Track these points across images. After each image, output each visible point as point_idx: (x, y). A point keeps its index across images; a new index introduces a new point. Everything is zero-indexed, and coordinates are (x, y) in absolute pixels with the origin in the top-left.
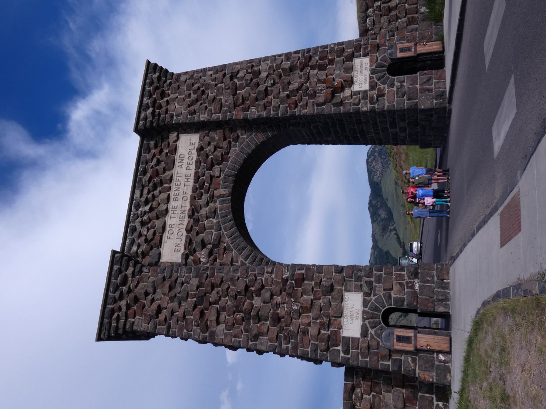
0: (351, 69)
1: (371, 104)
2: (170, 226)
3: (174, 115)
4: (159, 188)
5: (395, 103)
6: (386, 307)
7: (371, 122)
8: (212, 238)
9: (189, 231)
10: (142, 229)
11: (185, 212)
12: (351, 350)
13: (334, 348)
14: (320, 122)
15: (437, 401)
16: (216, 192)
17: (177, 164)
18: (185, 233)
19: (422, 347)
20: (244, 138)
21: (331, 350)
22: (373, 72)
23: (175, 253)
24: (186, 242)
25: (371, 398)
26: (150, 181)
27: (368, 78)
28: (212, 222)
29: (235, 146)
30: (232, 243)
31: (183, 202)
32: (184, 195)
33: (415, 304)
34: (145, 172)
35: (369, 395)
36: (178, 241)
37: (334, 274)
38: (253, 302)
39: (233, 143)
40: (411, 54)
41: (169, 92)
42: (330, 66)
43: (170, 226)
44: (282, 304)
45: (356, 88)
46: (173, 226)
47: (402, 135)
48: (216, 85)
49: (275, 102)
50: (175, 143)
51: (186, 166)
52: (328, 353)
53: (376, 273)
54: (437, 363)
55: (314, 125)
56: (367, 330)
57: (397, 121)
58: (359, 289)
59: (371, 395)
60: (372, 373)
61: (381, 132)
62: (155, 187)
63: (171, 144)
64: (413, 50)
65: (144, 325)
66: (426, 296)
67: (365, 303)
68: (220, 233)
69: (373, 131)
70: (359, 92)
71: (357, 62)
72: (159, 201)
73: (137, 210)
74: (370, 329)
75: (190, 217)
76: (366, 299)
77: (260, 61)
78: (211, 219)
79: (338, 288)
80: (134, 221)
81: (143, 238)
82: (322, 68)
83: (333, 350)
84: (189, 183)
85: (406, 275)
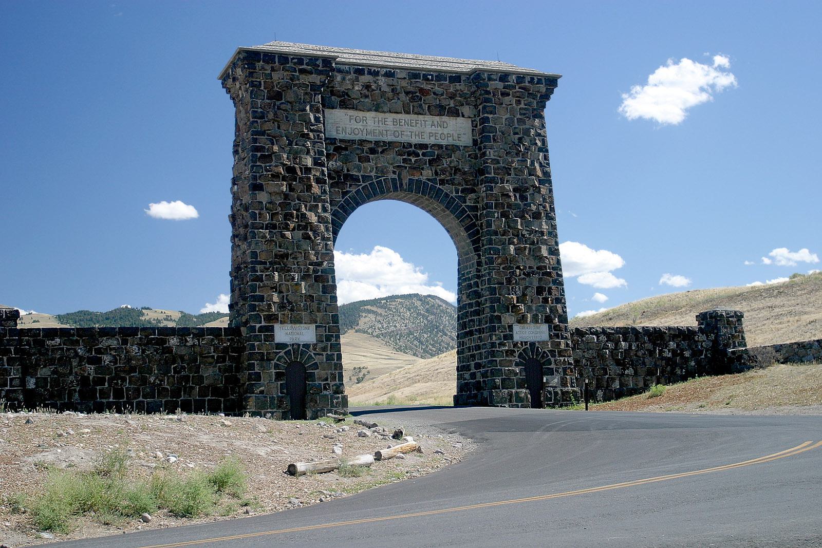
0: (535, 320)
1: (499, 344)
2: (365, 118)
3: (493, 115)
5: (499, 367)
7: (481, 344)
8: (354, 173)
11: (381, 136)
12: (263, 334)
16: (405, 171)
17: (437, 118)
18: (357, 138)
22: (532, 344)
23: (335, 128)
28: (371, 171)
29: (457, 192)
30: (349, 197)
31: (393, 132)
32: (400, 133)
35: (214, 352)
36: (348, 130)
37: (331, 314)
42: (541, 300)
43: (365, 118)
44: (297, 262)
45: (517, 328)
46: (364, 121)
47: (467, 376)
48: (526, 167)
49: (504, 240)
50: (461, 114)
51: (434, 132)
53: (334, 354)
54: (263, 412)
55: (480, 283)
56: (283, 349)
58: (319, 340)
59: (214, 354)
65: (259, 101)
67: (306, 346)
68: (360, 182)
71: (545, 327)
72: (393, 101)
75: (377, 143)
77: (550, 218)
78: (375, 169)
80: (370, 73)
81: (350, 87)
82: (540, 291)
83: (261, 317)
84: (413, 137)
85: (336, 382)
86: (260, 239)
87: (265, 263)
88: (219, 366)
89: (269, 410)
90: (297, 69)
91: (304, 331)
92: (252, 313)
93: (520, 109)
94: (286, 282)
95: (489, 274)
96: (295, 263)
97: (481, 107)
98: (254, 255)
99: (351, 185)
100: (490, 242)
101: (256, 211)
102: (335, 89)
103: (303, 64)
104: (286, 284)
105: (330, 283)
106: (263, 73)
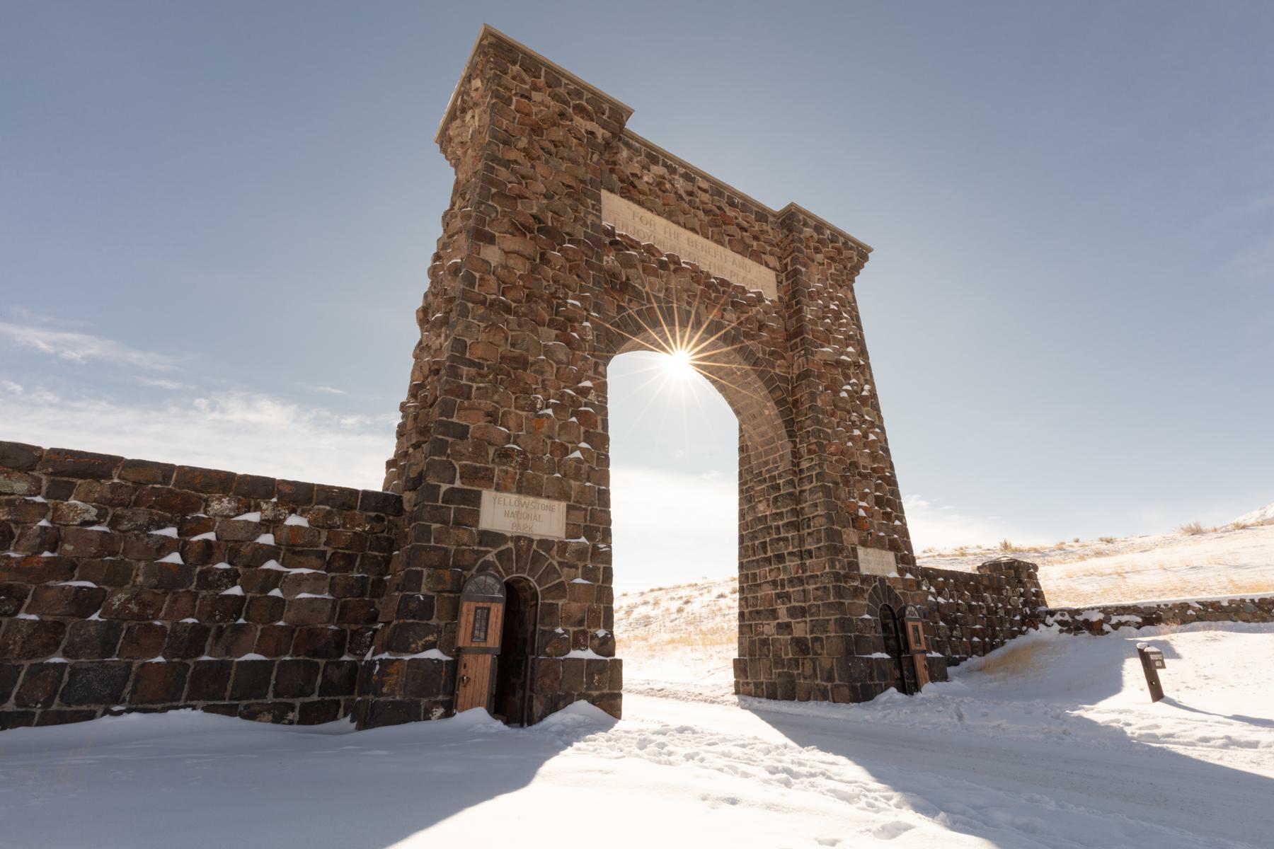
4: (706, 219)
6: (540, 587)
7: (805, 575)
8: (637, 285)
9: (650, 249)
10: (651, 175)
12: (453, 506)
13: (458, 471)
15: (303, 704)
17: (738, 257)
19: (465, 666)
20: (774, 368)
21: (453, 466)
22: (882, 580)
24: (632, 240)
25: (317, 547)
26: (719, 208)
27: (874, 574)
29: (764, 353)
33: (547, 650)
34: (732, 204)
35: (326, 544)
38: (546, 328)
39: (768, 349)
40: (913, 646)
41: (833, 271)
44: (543, 381)
52: (448, 457)
53: (599, 568)
55: (796, 482)
56: (494, 546)
59: (326, 548)
60: (377, 553)
61: (777, 591)
62: (706, 212)
63: (763, 256)
64: (918, 648)
66: (564, 672)
67: (546, 544)
69: (781, 577)
70: (856, 556)
73: (681, 176)
74: (496, 551)
76: (553, 546)
79: (573, 493)
80: (665, 165)
81: (639, 173)
83: (455, 470)
86: (475, 321)
87: (480, 366)
88: (333, 578)
89: (441, 698)
90: (571, 104)
91: (544, 514)
92: (436, 458)
93: (831, 274)
94: (518, 411)
95: (820, 466)
96: (540, 381)
97: (789, 260)
98: (460, 345)
99: (630, 301)
100: (818, 422)
101: (474, 273)
102: (617, 167)
103: (581, 98)
104: (517, 414)
105: (600, 430)
106: (517, 86)
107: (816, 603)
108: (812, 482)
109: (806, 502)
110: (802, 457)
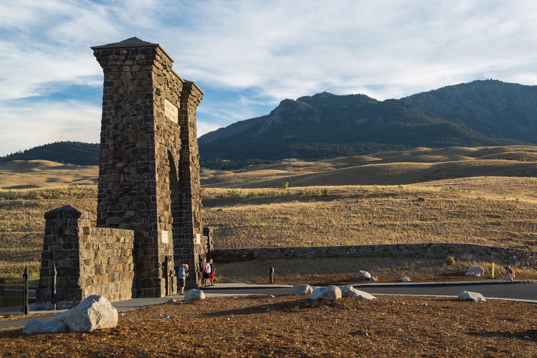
7: (180, 244)
14: (180, 212)
57: (179, 260)
107: (184, 254)
108: (187, 209)
109: (183, 216)
110: (183, 198)
